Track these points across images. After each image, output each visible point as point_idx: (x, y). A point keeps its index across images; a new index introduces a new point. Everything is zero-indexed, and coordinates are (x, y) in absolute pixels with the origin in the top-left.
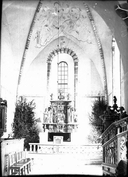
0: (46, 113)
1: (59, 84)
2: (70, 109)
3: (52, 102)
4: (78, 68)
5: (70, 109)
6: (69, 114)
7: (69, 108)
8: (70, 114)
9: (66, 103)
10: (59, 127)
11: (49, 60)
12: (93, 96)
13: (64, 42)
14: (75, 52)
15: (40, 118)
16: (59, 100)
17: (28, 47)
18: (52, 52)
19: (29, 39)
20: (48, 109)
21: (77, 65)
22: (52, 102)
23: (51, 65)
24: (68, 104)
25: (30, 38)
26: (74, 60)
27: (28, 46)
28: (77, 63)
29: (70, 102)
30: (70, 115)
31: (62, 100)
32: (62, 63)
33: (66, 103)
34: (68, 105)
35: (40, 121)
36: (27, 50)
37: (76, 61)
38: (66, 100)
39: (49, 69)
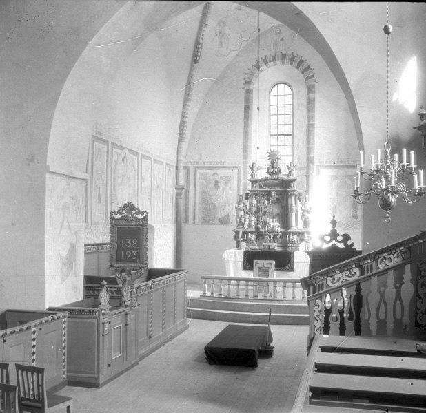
0: (242, 206)
1: (271, 135)
2: (293, 198)
3: (253, 182)
4: (314, 99)
5: (293, 198)
6: (291, 207)
7: (291, 195)
8: (294, 208)
9: (286, 184)
10: (270, 238)
11: (248, 82)
12: (350, 163)
13: (282, 39)
14: (308, 62)
15: (228, 216)
16: (268, 176)
17: (198, 58)
18: (255, 63)
19: (201, 41)
20: (244, 197)
21: (314, 92)
22: (253, 182)
23: (252, 93)
24: (290, 186)
25: (202, 39)
26: (306, 79)
27: (199, 56)
28: (313, 86)
29: (293, 181)
30: (294, 211)
31: (276, 176)
32: (279, 85)
33: (286, 184)
34: (290, 189)
35: (230, 223)
36: (197, 65)
37: (311, 82)
38: (283, 175)
39: (248, 103)
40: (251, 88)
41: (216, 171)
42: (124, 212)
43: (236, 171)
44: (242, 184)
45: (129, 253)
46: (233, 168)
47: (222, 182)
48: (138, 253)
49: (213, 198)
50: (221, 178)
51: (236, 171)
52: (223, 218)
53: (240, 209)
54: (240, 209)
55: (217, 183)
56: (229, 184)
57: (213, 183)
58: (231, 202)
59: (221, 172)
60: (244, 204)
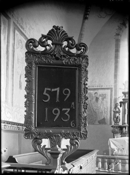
0: (117, 110)
15: (104, 119)
39: (118, 47)
40: (119, 38)
41: (96, 91)
42: (50, 42)
43: (109, 91)
44: (113, 99)
45: (67, 92)
46: (108, 89)
47: (100, 98)
48: (73, 112)
49: (95, 108)
50: (100, 95)
51: (109, 91)
52: (101, 120)
53: (117, 112)
54: (117, 112)
55: (97, 99)
56: (105, 99)
57: (94, 100)
58: (106, 110)
59: (100, 92)
60: (119, 109)
